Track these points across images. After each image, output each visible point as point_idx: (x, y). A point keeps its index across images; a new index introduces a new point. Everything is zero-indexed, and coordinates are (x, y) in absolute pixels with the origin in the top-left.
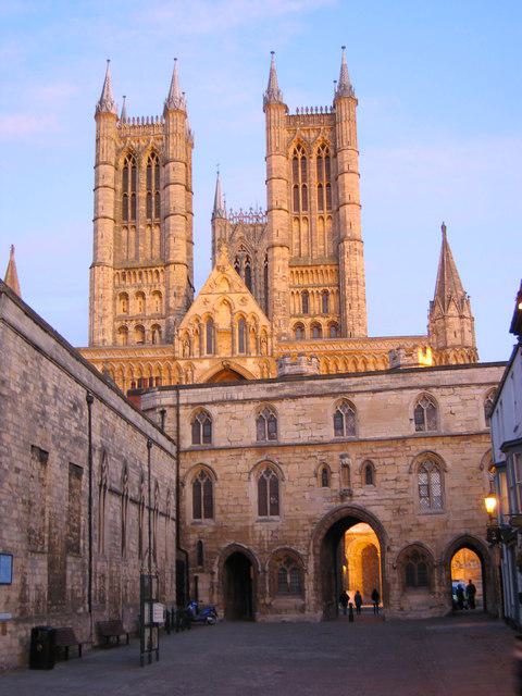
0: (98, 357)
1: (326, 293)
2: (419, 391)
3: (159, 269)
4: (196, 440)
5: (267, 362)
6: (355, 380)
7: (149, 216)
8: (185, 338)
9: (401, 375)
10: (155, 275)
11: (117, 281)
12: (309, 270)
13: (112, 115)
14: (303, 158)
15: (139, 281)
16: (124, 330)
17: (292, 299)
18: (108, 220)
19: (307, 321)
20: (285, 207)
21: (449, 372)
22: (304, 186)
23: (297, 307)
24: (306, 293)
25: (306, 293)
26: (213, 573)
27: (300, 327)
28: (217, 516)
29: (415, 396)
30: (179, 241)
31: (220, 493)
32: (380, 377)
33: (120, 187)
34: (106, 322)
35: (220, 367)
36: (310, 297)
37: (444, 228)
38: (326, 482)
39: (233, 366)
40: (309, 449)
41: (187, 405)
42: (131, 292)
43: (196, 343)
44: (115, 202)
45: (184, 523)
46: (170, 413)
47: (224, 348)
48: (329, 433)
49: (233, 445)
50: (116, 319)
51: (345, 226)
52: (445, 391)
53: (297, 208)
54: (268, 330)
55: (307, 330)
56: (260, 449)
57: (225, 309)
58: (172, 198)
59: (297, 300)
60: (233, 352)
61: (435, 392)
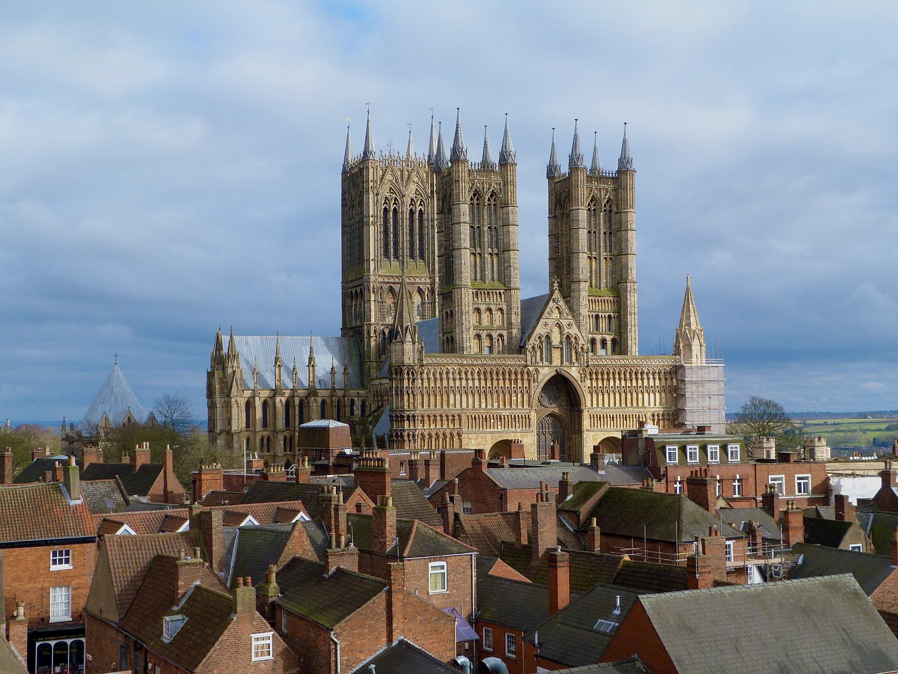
0: (475, 362)
1: (610, 316)
3: (502, 291)
10: (498, 295)
12: (600, 299)
15: (487, 300)
16: (478, 336)
19: (598, 338)
20: (586, 251)
23: (592, 326)
24: (597, 317)
25: (597, 316)
27: (593, 341)
36: (600, 319)
42: (483, 307)
43: (538, 354)
54: (585, 347)
55: (599, 345)
59: (591, 321)
60: (562, 362)
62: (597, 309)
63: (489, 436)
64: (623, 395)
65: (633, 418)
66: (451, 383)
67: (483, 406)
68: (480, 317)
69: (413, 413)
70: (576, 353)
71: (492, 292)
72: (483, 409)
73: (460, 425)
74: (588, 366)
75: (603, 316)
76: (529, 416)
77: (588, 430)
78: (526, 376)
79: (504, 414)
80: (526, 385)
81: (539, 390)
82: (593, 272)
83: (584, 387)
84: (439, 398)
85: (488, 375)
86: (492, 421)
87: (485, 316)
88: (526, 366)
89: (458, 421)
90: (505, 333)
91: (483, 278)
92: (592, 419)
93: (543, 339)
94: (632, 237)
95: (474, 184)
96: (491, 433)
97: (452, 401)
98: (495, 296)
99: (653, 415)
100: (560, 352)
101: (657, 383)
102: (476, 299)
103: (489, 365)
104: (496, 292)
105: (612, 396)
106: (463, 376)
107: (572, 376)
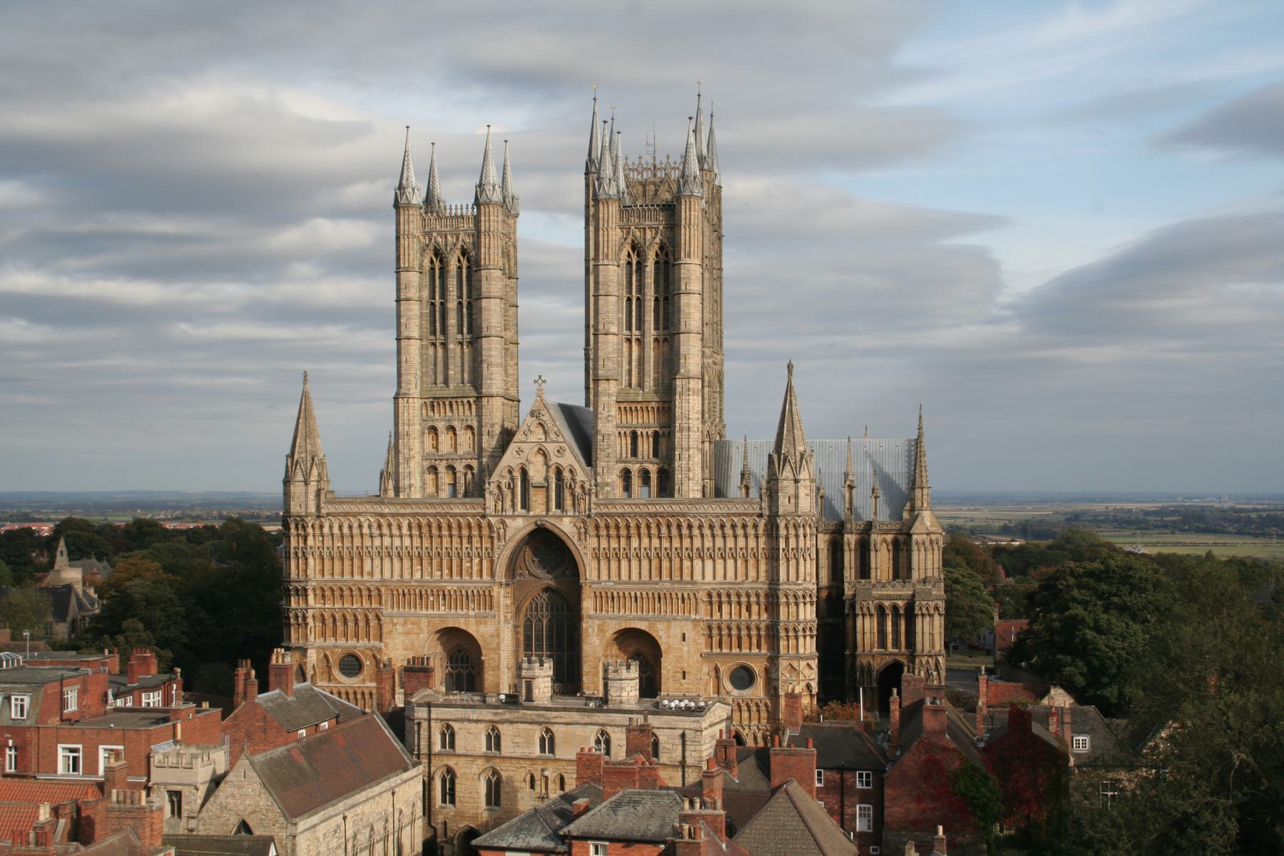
0: (402, 511)
2: (598, 727)
3: (471, 400)
4: (444, 746)
5: (584, 522)
6: (554, 714)
7: (461, 332)
8: (496, 491)
9: (586, 714)
10: (467, 406)
11: (424, 412)
14: (638, 263)
15: (449, 413)
16: (433, 469)
17: (618, 440)
18: (412, 342)
20: (614, 329)
21: (619, 715)
22: (638, 299)
23: (624, 449)
24: (634, 436)
26: (454, 845)
27: (626, 475)
28: (457, 804)
29: (595, 731)
30: (494, 369)
31: (458, 787)
32: (572, 713)
33: (426, 293)
34: (412, 464)
36: (640, 439)
37: (790, 367)
38: (532, 787)
39: (548, 526)
40: (522, 761)
41: (437, 719)
42: (441, 426)
44: (422, 315)
45: (435, 806)
46: (425, 724)
47: (538, 508)
48: (536, 751)
49: (469, 753)
50: (424, 458)
51: (679, 359)
52: (616, 729)
53: (629, 328)
54: (587, 486)
55: (636, 481)
56: (487, 758)
57: (540, 458)
58: (485, 315)
59: (624, 442)
60: (548, 510)
61: (609, 729)
62: (635, 422)
64: (655, 563)
66: (368, 542)
67: (417, 576)
68: (437, 440)
69: (303, 584)
70: (573, 495)
71: (457, 402)
72: (415, 582)
73: (380, 604)
74: (589, 516)
75: (644, 433)
76: (490, 592)
77: (590, 617)
78: (485, 532)
79: (449, 588)
80: (486, 544)
81: (507, 553)
82: (634, 364)
83: (585, 550)
84: (347, 563)
85: (425, 530)
86: (431, 598)
87: (445, 439)
88: (484, 516)
89: (378, 598)
90: (475, 463)
91: (446, 382)
93: (517, 474)
94: (688, 305)
95: (430, 239)
96: (427, 616)
97: (367, 567)
98: (461, 408)
99: (710, 595)
100: (545, 494)
101: (752, 543)
102: (431, 414)
103: (424, 515)
104: (462, 402)
105: (634, 563)
106: (385, 530)
107: (565, 533)
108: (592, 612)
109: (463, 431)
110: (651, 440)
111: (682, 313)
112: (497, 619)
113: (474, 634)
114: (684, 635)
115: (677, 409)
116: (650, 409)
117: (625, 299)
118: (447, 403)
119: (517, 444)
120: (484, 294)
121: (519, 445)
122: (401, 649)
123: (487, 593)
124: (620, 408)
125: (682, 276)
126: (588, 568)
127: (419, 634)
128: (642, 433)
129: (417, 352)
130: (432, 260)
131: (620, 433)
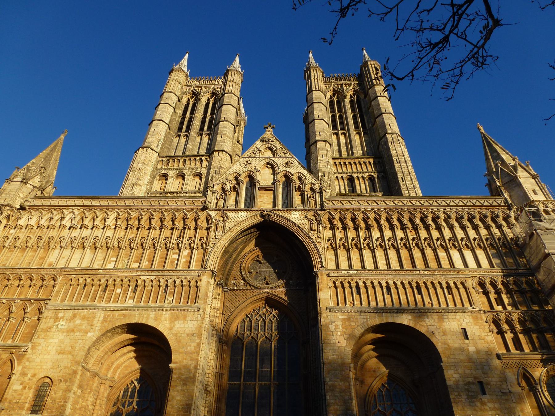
3: (203, 158)
5: (316, 215)
7: (202, 129)
13: (183, 71)
14: (338, 102)
15: (181, 166)
17: (336, 182)
24: (351, 180)
33: (180, 112)
35: (258, 219)
36: (356, 181)
39: (274, 218)
42: (172, 173)
54: (317, 187)
63: (100, 315)
64: (404, 253)
65: (435, 289)
70: (302, 195)
74: (322, 209)
81: (224, 242)
86: (119, 290)
92: (340, 290)
96: (105, 309)
100: (272, 196)
104: (195, 159)
108: (332, 305)
109: (191, 177)
110: (367, 182)
111: (381, 105)
112: (201, 312)
113: (165, 333)
114: (465, 329)
115: (391, 150)
116: (362, 163)
117: (330, 116)
118: (182, 160)
119: (245, 159)
120: (222, 119)
121: (248, 159)
122: (53, 353)
123: (193, 284)
124: (335, 163)
125: (376, 90)
126: (323, 257)
127: (86, 332)
128: (357, 176)
129: (165, 130)
130: (189, 99)
131: (337, 177)
